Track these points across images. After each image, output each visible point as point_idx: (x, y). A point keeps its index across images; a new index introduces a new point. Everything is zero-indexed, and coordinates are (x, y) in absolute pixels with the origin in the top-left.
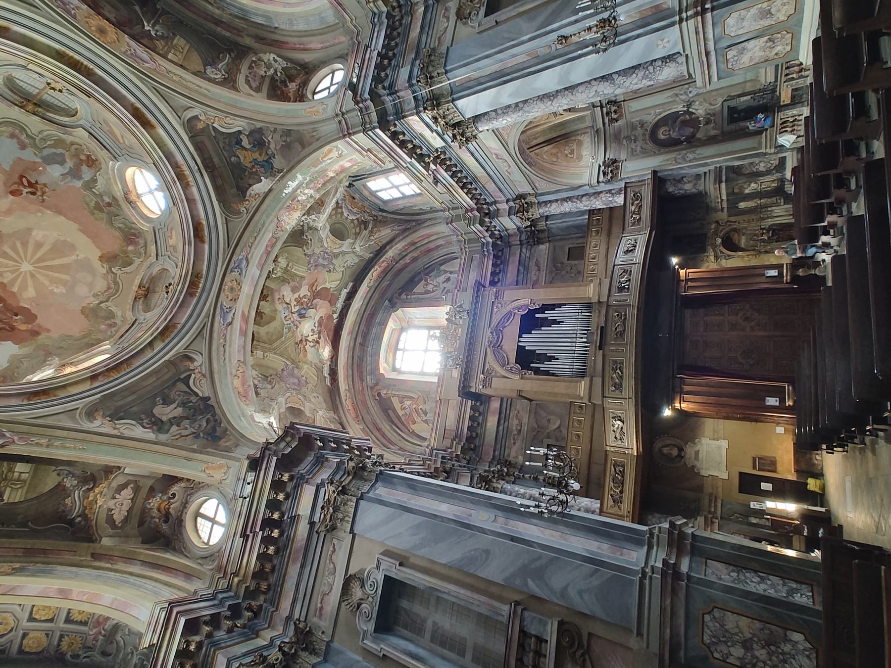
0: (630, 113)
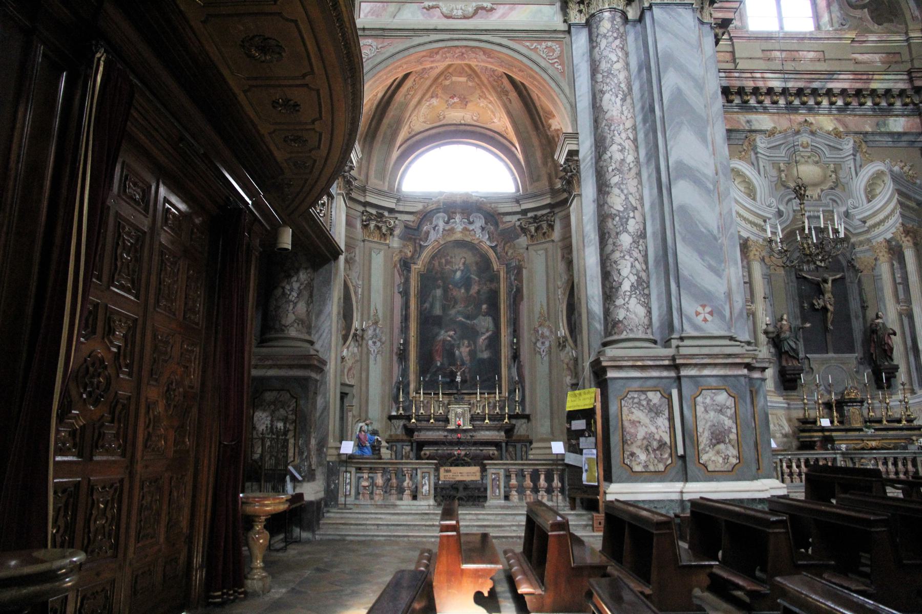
0: (370, 249)
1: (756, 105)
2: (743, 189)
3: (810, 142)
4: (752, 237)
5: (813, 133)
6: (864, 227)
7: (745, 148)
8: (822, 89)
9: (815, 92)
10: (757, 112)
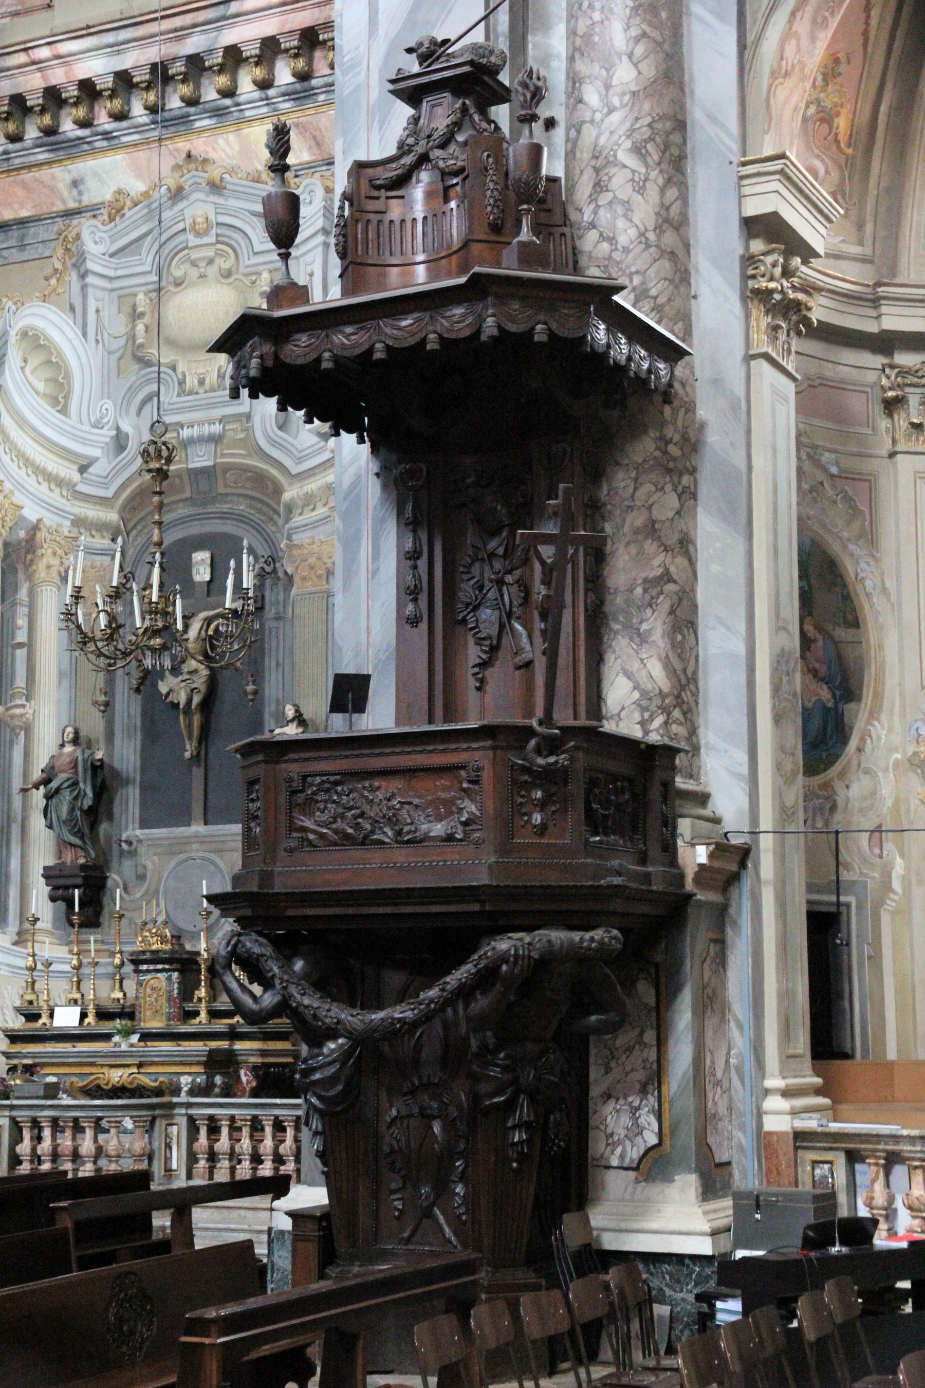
1: (81, 133)
2: (41, 386)
3: (212, 217)
4: (50, 520)
5: (216, 187)
6: (322, 450)
7: (58, 265)
8: (210, 51)
9: (196, 63)
10: (94, 152)
